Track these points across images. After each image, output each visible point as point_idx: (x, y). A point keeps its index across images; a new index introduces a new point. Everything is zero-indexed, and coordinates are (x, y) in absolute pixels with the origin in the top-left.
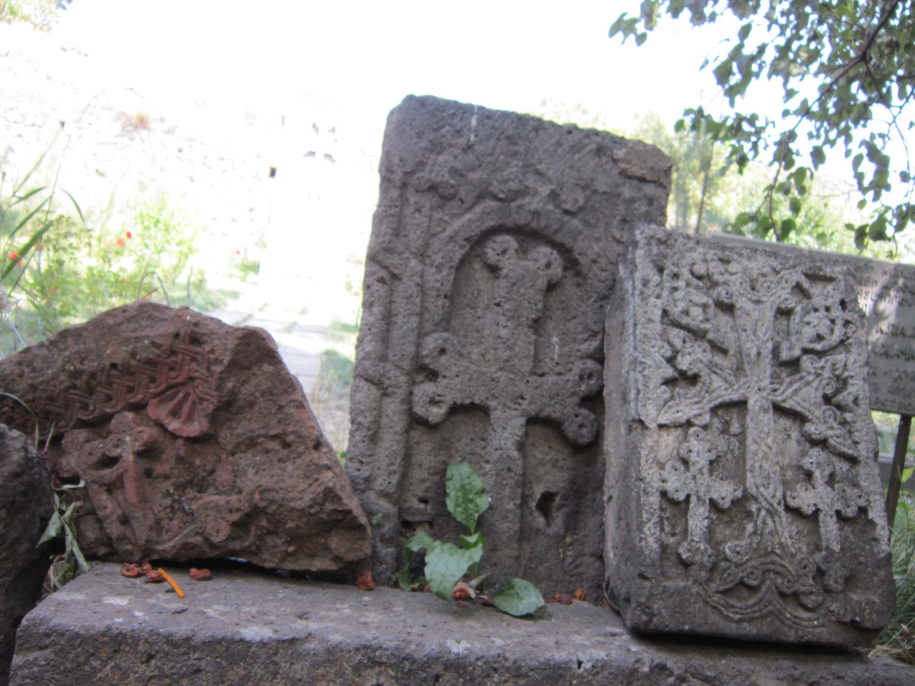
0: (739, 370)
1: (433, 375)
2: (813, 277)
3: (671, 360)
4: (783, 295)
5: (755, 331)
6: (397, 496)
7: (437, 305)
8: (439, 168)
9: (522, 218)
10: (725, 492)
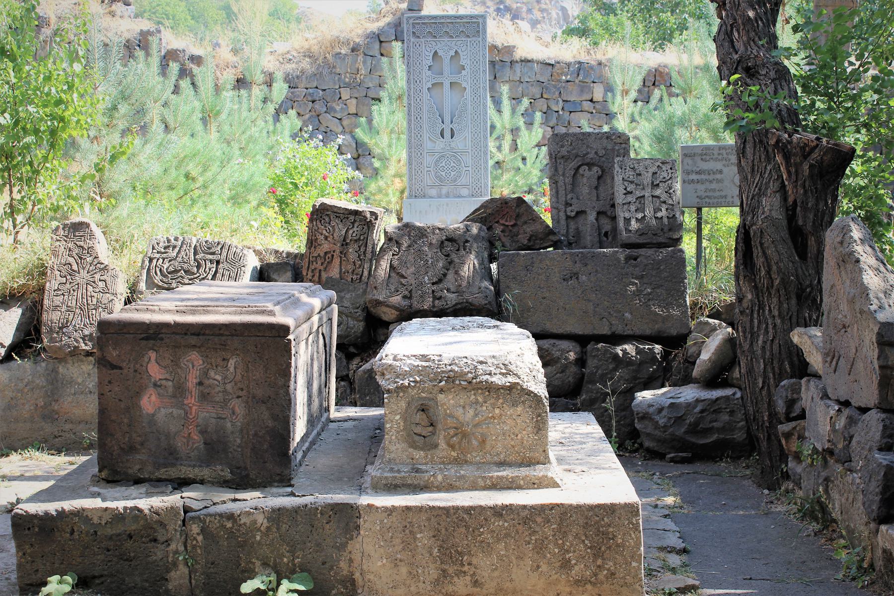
0: (643, 189)
1: (571, 205)
2: (663, 163)
3: (625, 189)
4: (655, 169)
5: (647, 178)
6: (567, 235)
7: (569, 187)
8: (564, 152)
9: (588, 161)
10: (640, 216)
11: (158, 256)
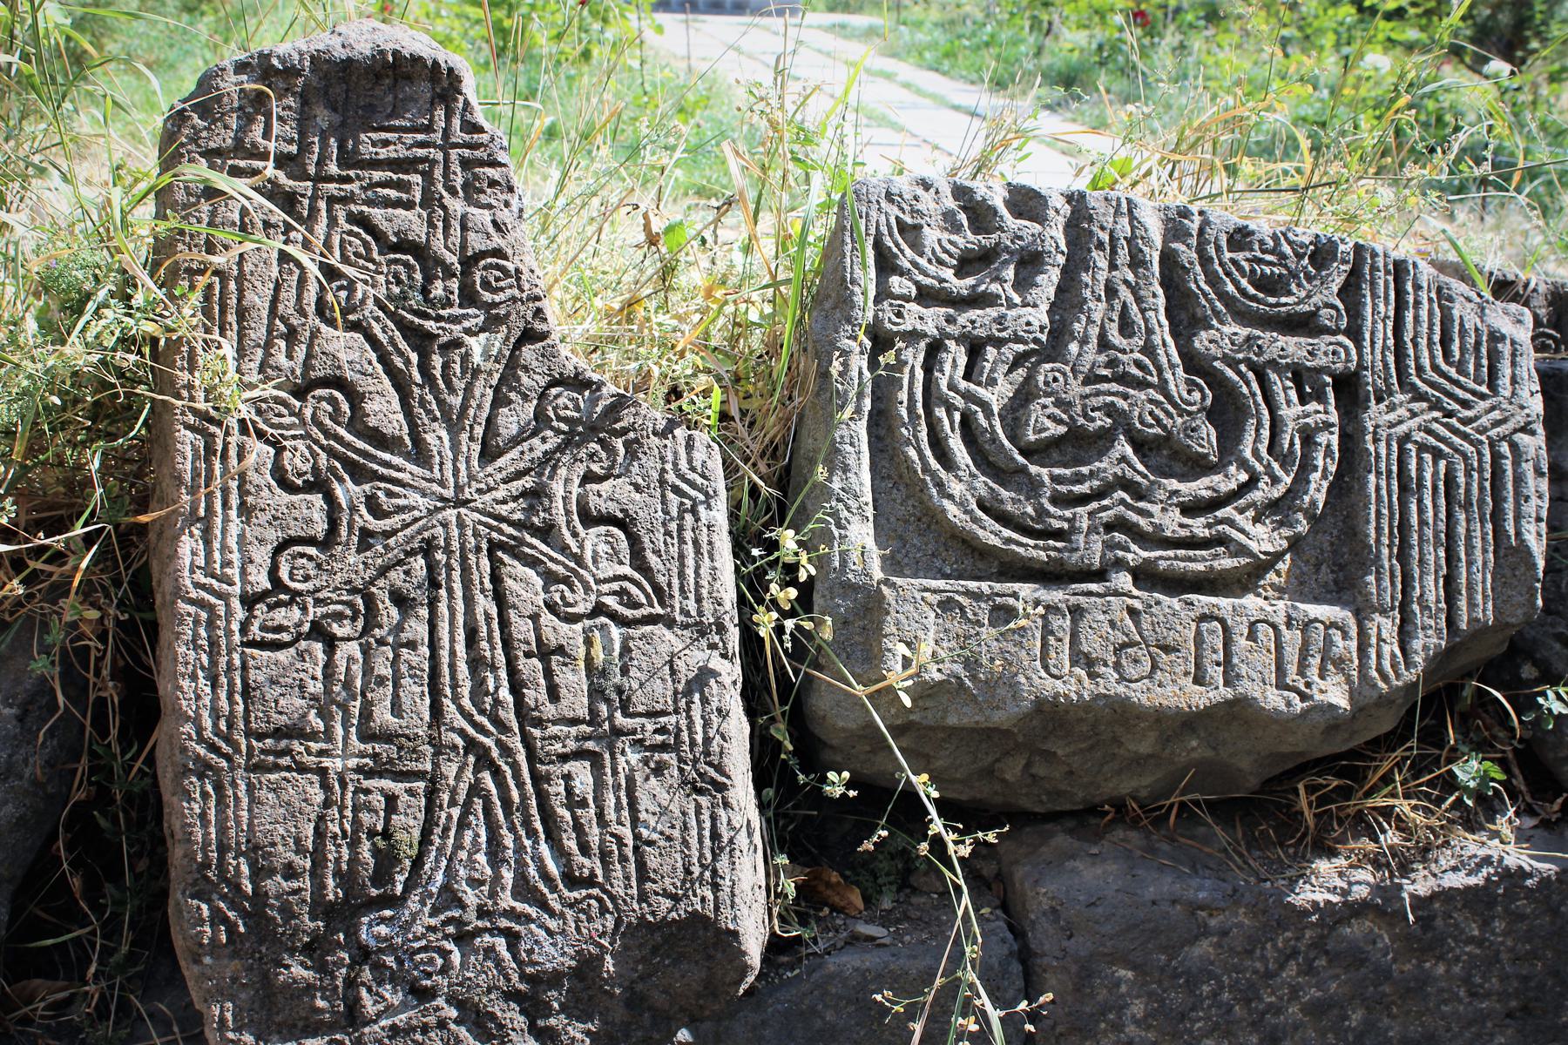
11: (930, 319)
